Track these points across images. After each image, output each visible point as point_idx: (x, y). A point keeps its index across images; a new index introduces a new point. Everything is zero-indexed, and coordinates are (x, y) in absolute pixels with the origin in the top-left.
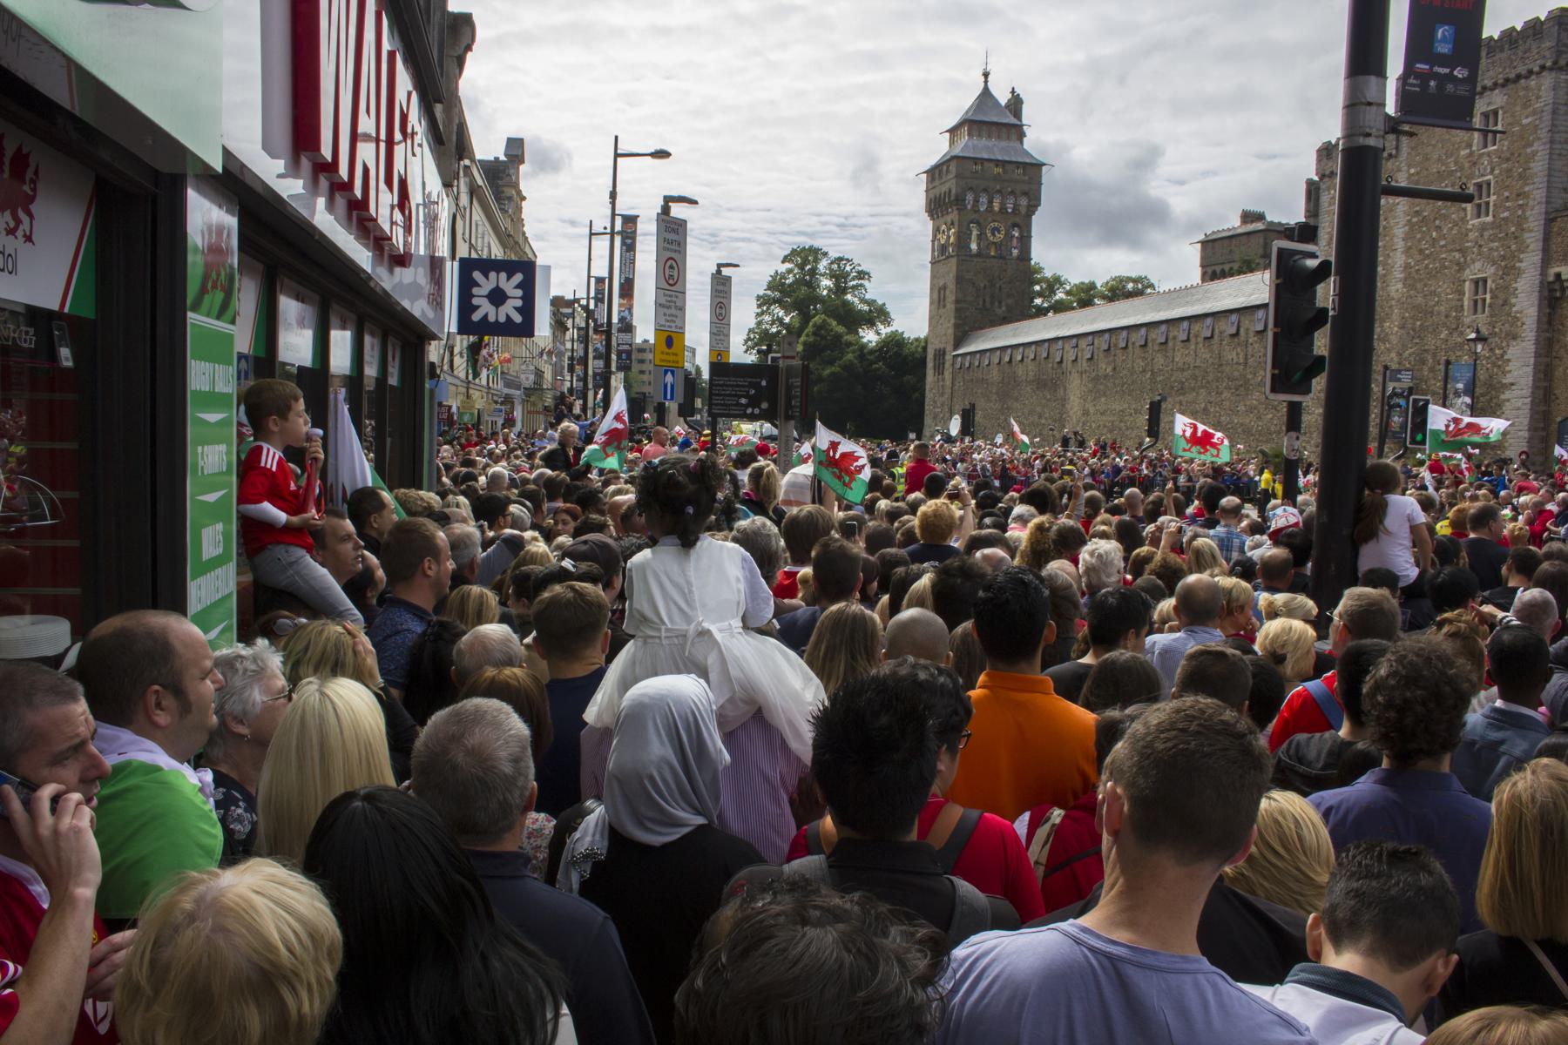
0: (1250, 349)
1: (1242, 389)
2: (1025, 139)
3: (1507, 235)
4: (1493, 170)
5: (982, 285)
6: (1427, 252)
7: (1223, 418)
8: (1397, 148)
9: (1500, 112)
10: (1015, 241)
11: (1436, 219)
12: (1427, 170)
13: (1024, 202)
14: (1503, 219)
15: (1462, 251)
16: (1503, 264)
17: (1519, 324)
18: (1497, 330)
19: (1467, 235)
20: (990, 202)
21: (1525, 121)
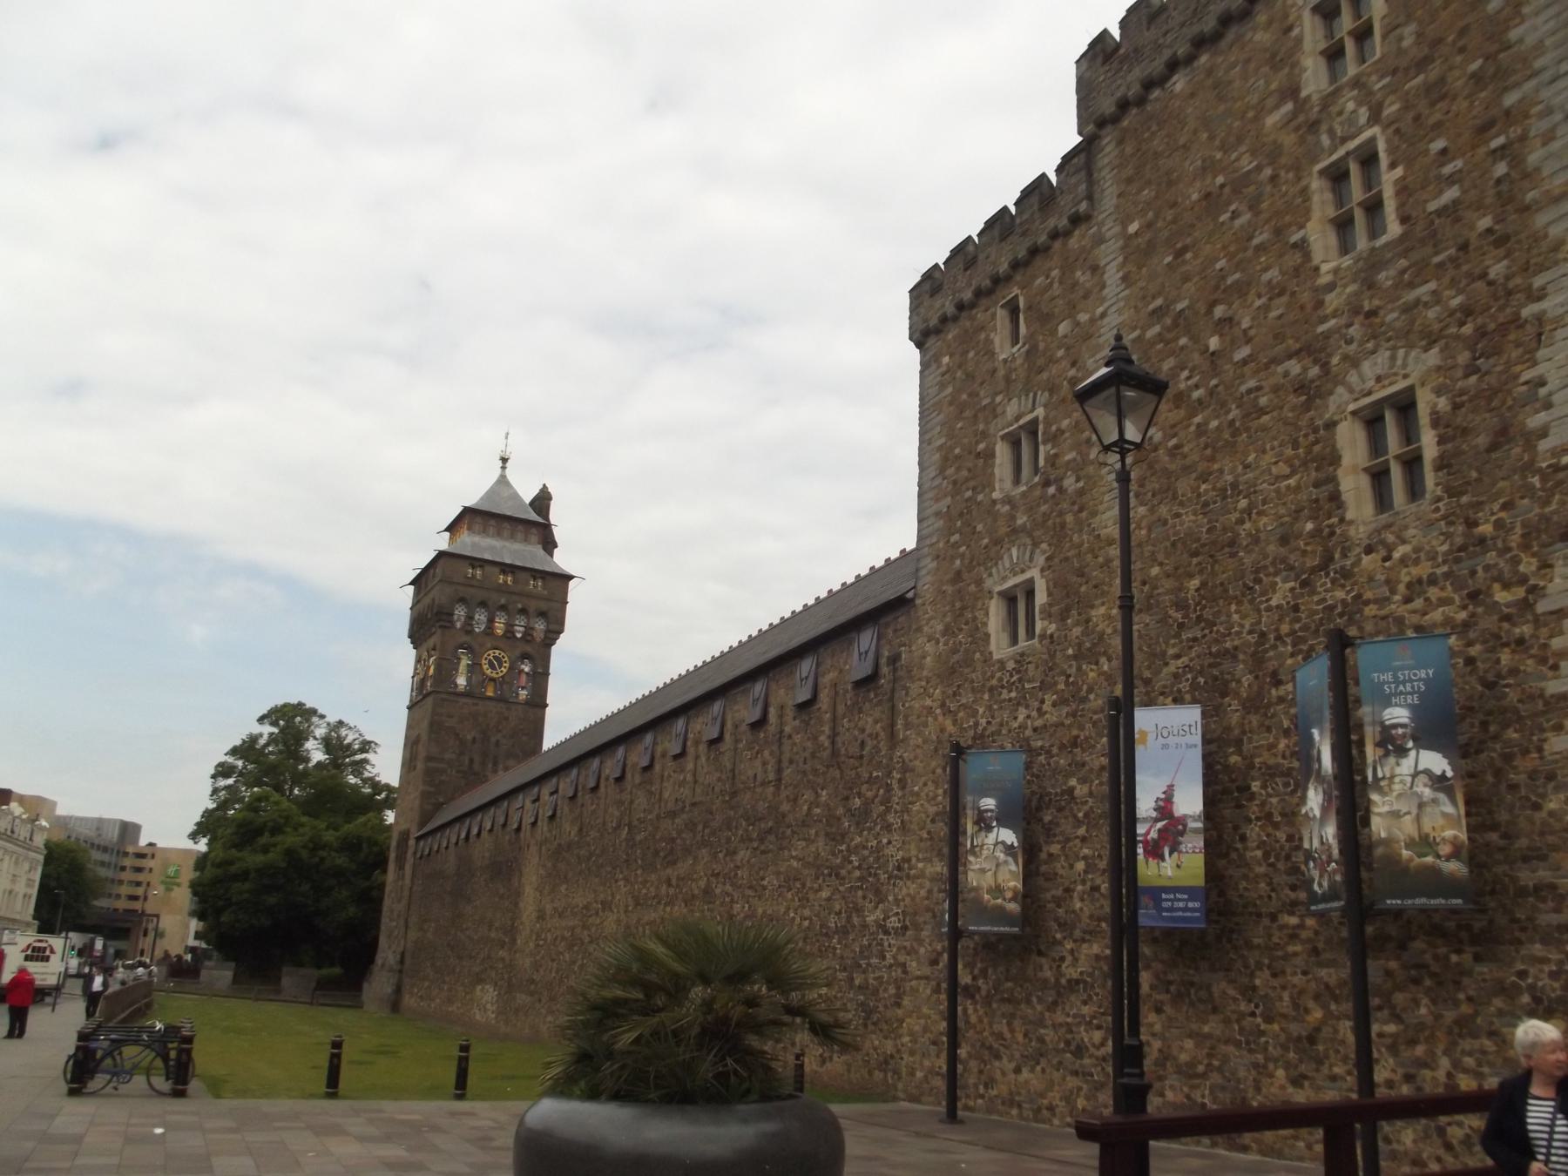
0: (786, 747)
1: (772, 838)
2: (556, 551)
3: (1464, 247)
4: (1374, 118)
5: (469, 737)
6: (1196, 394)
7: (737, 907)
8: (1090, 197)
10: (524, 677)
11: (1213, 304)
12: (1174, 205)
13: (540, 626)
14: (1439, 213)
15: (1314, 350)
16: (1467, 329)
18: (1486, 529)
19: (1320, 304)
20: (491, 621)
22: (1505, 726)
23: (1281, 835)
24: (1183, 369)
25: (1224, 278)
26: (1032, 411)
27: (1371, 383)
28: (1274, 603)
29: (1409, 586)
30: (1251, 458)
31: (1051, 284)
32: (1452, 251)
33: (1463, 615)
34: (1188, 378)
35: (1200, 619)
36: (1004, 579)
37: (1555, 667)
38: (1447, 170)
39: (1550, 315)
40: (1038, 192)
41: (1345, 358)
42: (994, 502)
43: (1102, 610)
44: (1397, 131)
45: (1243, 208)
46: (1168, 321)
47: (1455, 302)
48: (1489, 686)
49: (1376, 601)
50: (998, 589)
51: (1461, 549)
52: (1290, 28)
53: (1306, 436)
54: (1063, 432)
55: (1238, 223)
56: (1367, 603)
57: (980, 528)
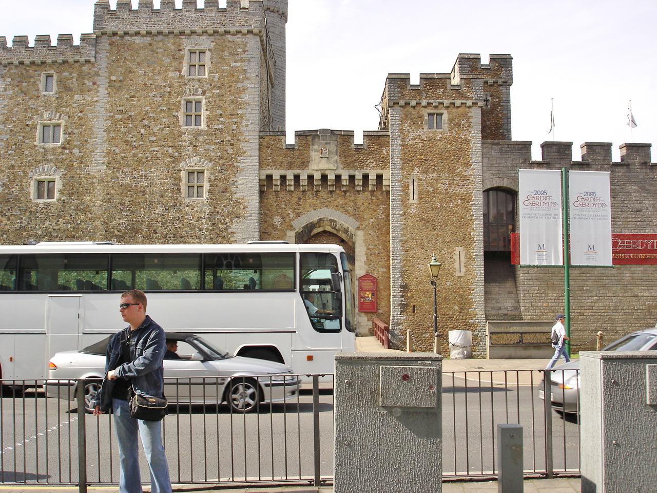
4: (204, 93)
9: (208, 54)
11: (144, 119)
21: (233, 64)
26: (59, 119)
27: (193, 164)
29: (198, 218)
30: (152, 170)
31: (72, 78)
33: (211, 228)
35: (129, 210)
36: (40, 175)
40: (65, 39)
42: (35, 146)
43: (89, 198)
46: (126, 116)
50: (34, 177)
52: (180, 50)
54: (74, 134)
56: (186, 219)
57: (26, 152)
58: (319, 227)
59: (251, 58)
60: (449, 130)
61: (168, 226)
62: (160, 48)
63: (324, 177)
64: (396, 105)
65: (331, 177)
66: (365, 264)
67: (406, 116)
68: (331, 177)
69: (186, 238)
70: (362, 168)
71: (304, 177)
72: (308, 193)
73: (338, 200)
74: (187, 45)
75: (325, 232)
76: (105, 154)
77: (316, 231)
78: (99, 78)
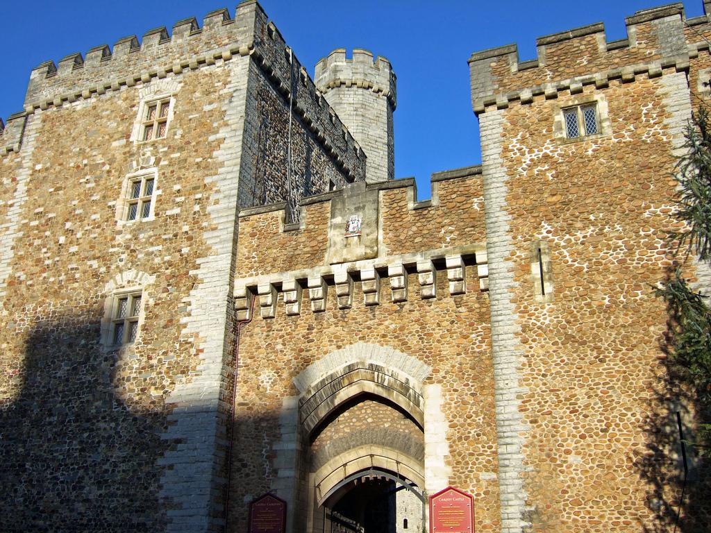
3: (176, 236)
6: (47, 262)
11: (67, 220)
15: (104, 258)
16: (168, 272)
17: (193, 351)
18: (154, 362)
19: (113, 239)
21: (207, 108)
22: (142, 450)
23: (34, 491)
24: (45, 247)
25: (75, 210)
27: (125, 283)
28: (58, 375)
32: (171, 236)
34: (45, 253)
37: (166, 428)
38: (178, 200)
39: (200, 277)
41: (118, 267)
44: (164, 174)
45: (92, 180)
46: (43, 221)
47: (167, 258)
48: (140, 432)
49: (103, 384)
51: (143, 368)
52: (134, 106)
53: (92, 298)
55: (88, 186)
56: (99, 384)
58: (350, 384)
59: (234, 91)
60: (614, 132)
61: (70, 400)
62: (107, 110)
63: (355, 276)
64: (491, 108)
65: (367, 270)
66: (448, 463)
67: (513, 123)
68: (367, 270)
69: (95, 421)
70: (430, 247)
71: (314, 280)
72: (327, 314)
73: (386, 323)
74: (145, 94)
75: (364, 396)
76: (5, 285)
77: (344, 394)
78: (21, 170)
